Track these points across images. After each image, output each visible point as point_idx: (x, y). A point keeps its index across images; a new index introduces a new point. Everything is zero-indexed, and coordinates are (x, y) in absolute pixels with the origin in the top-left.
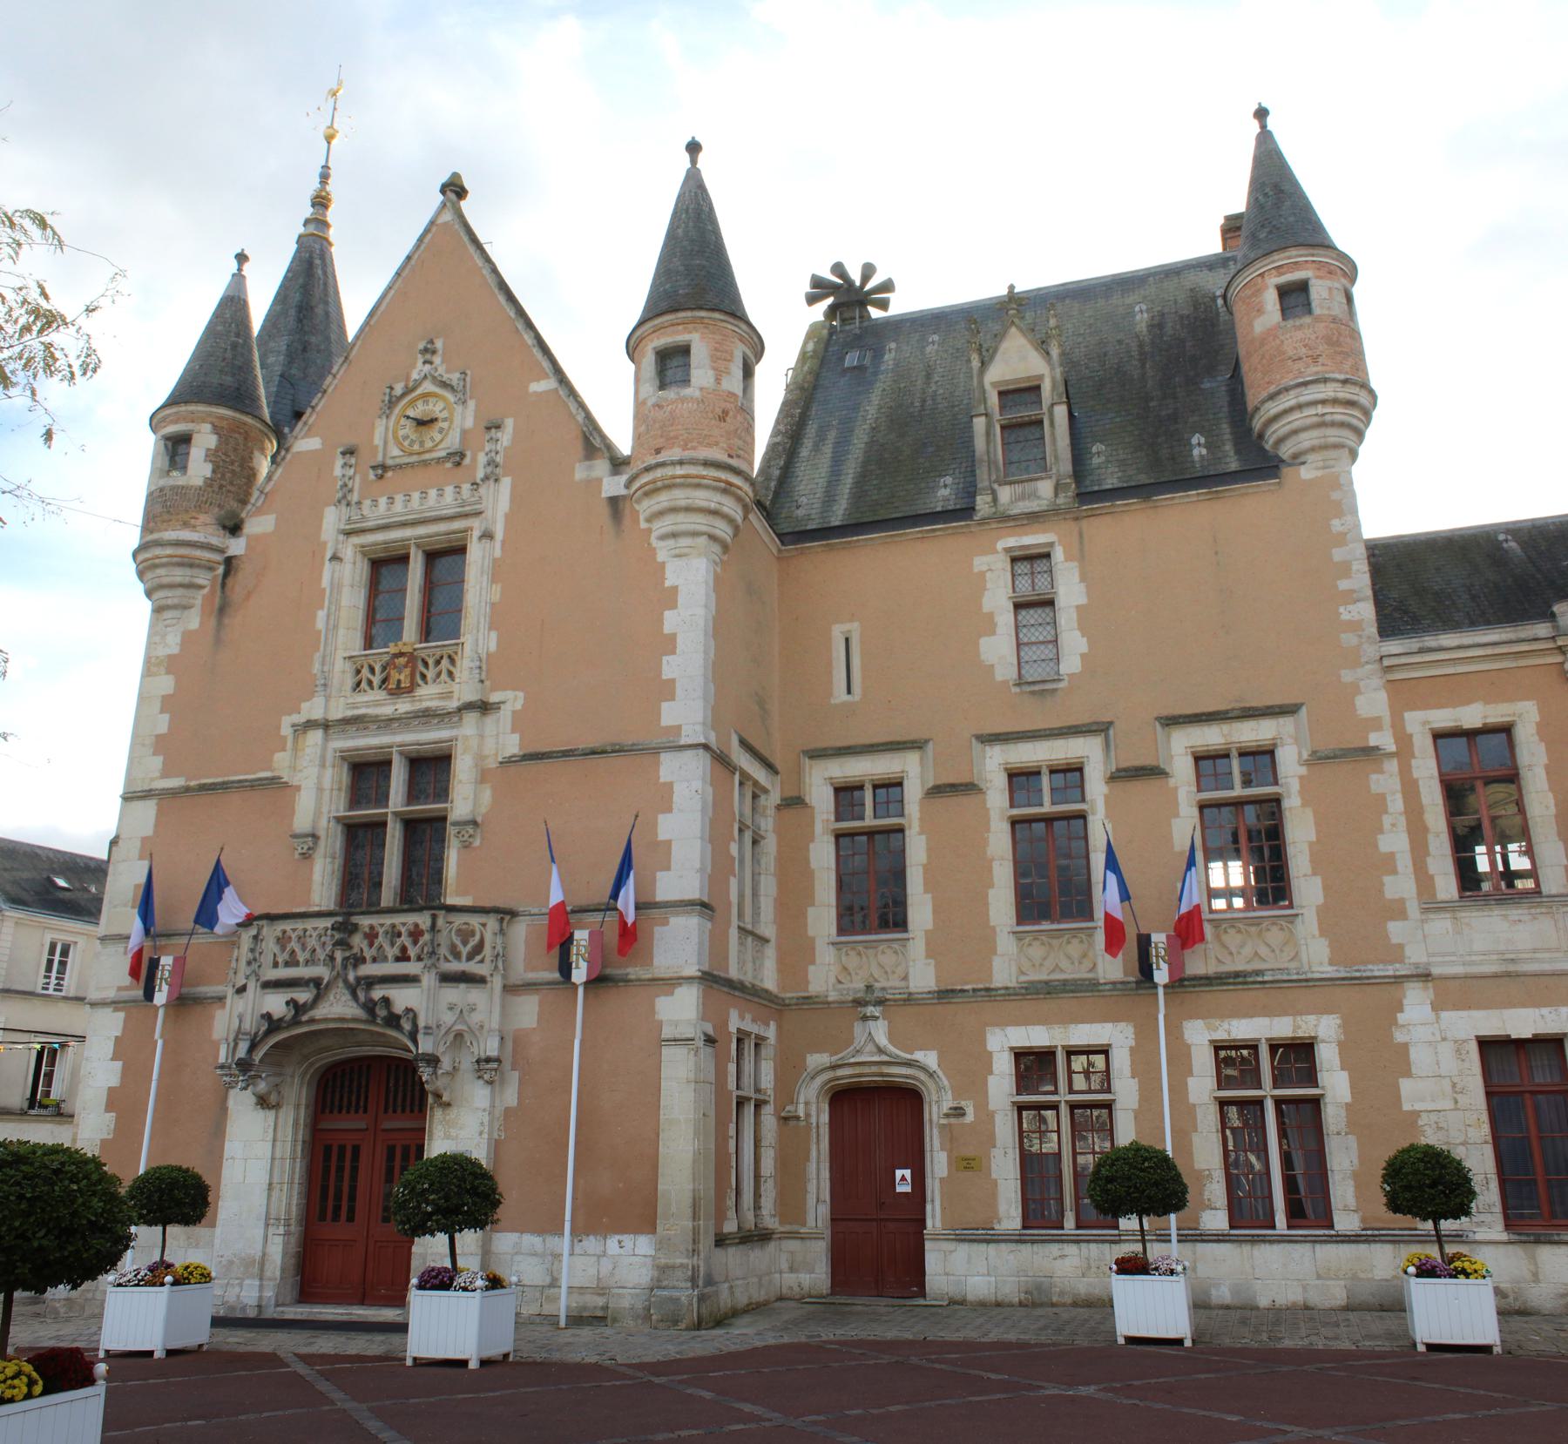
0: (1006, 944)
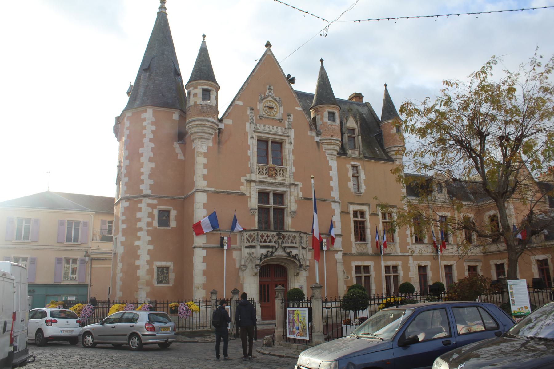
0: (354, 245)
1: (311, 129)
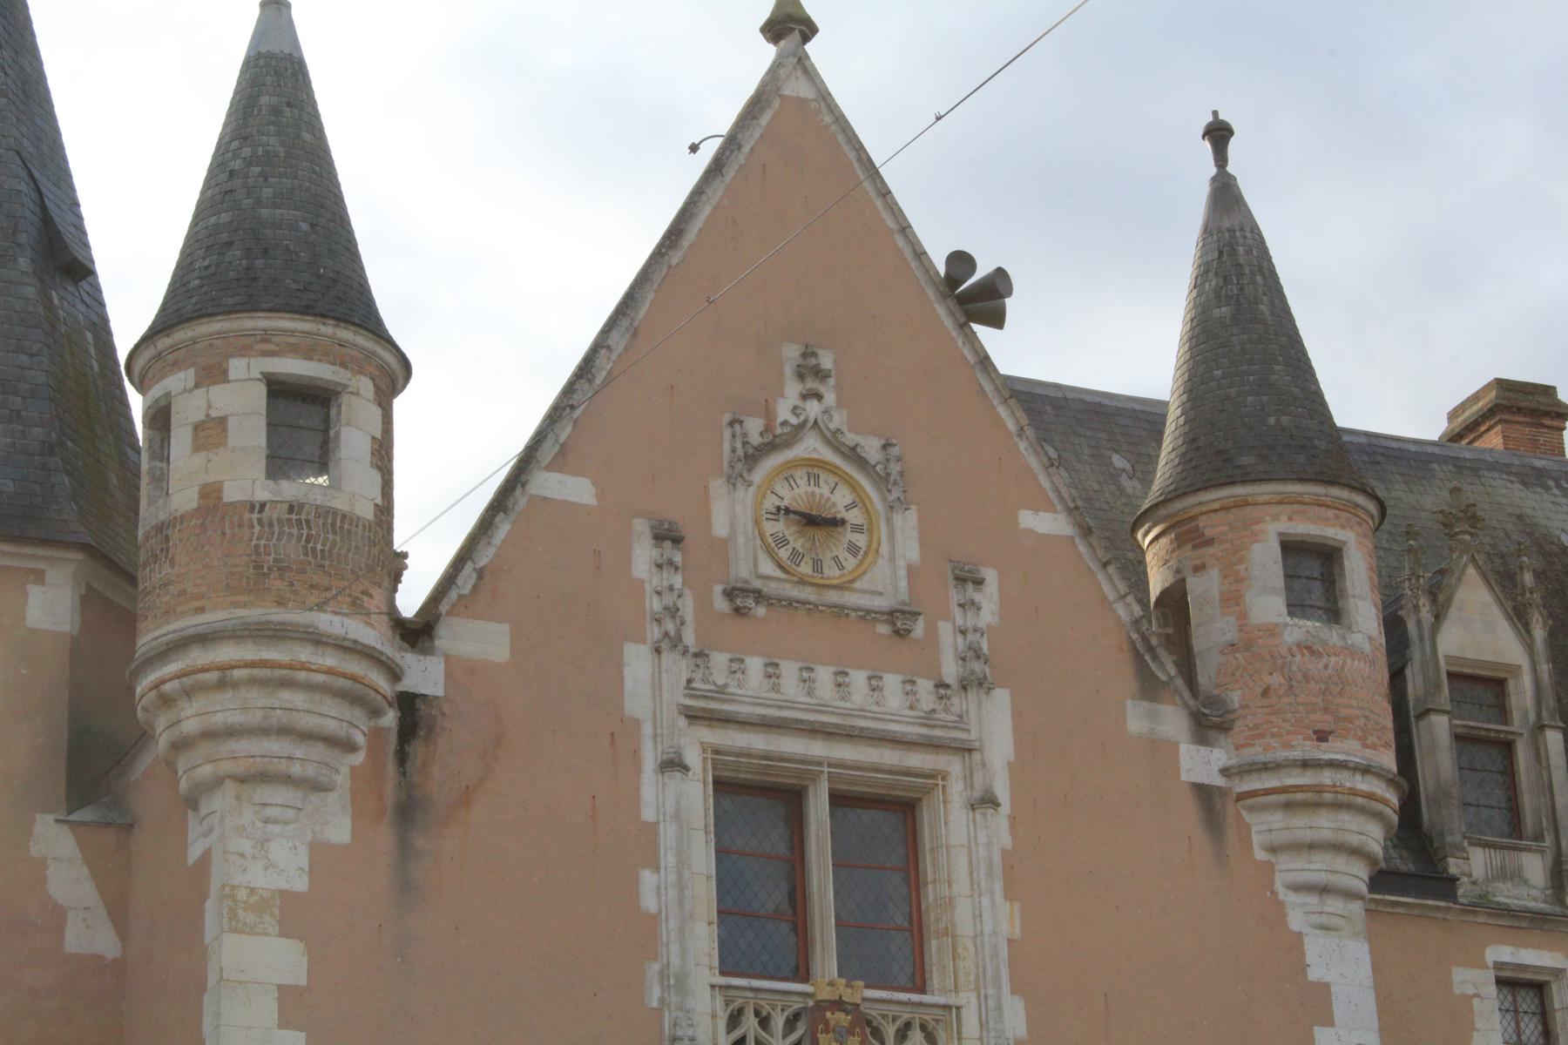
1: (1150, 688)
